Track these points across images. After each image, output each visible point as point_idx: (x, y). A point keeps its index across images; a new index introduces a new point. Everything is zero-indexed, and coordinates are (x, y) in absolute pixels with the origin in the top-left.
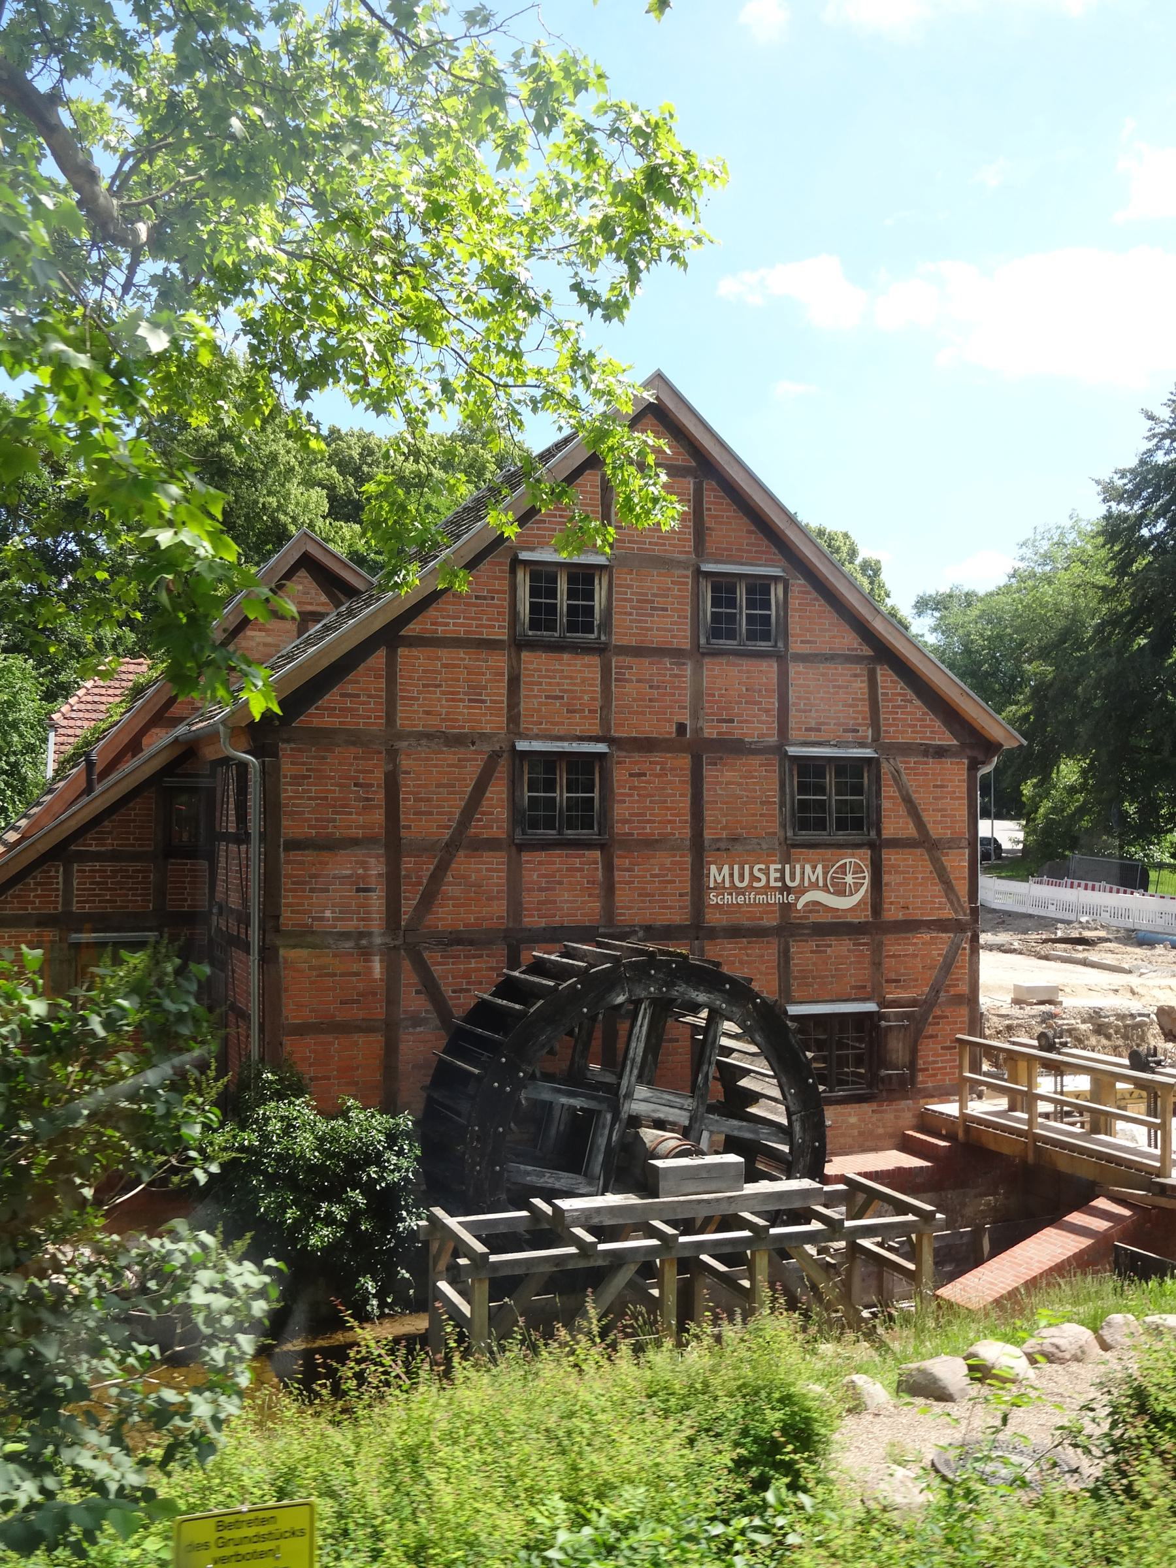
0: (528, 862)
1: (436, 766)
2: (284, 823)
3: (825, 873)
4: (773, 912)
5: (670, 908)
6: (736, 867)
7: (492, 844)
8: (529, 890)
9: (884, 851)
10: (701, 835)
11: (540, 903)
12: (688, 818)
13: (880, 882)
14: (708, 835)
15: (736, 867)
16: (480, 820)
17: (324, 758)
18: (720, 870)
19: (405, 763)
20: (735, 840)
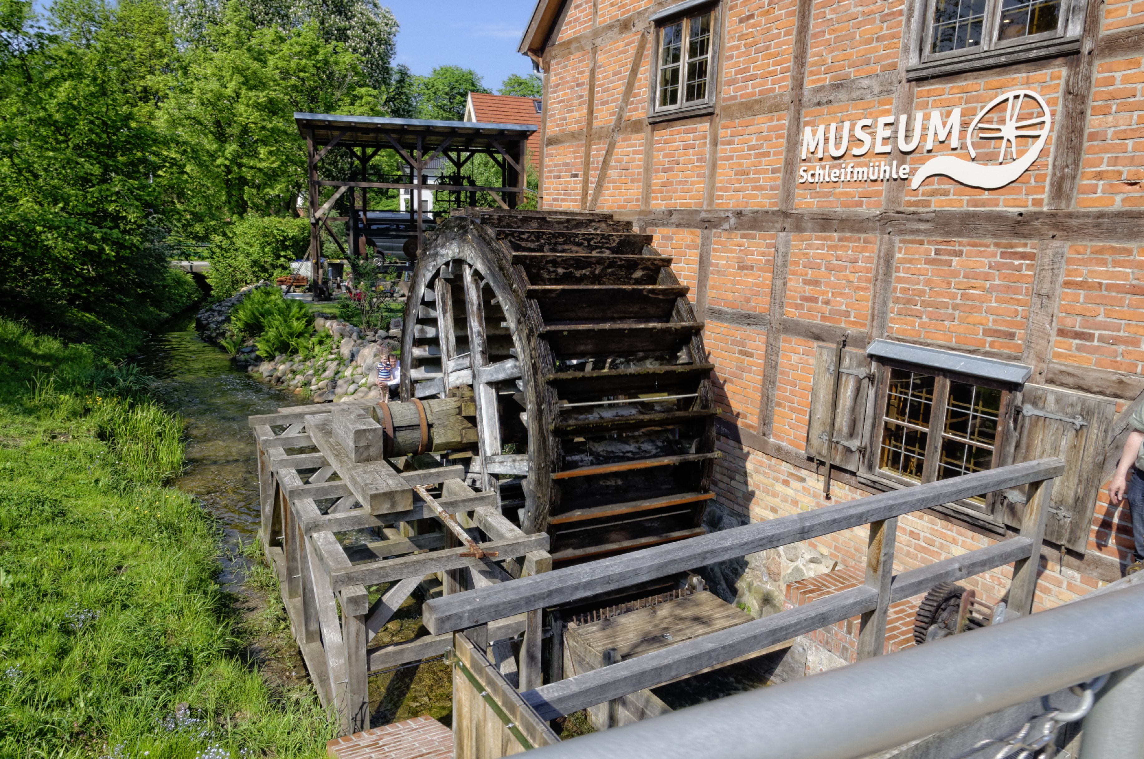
0: (658, 142)
1: (613, 56)
2: (548, 124)
3: (965, 125)
4: (878, 194)
5: (761, 188)
6: (833, 126)
7: (636, 126)
8: (657, 171)
9: (1097, 63)
10: (801, 86)
11: (664, 185)
12: (790, 64)
13: (1081, 131)
14: (808, 86)
15: (833, 126)
16: (632, 103)
17: (566, 66)
18: (814, 133)
19: (601, 57)
20: (836, 87)
